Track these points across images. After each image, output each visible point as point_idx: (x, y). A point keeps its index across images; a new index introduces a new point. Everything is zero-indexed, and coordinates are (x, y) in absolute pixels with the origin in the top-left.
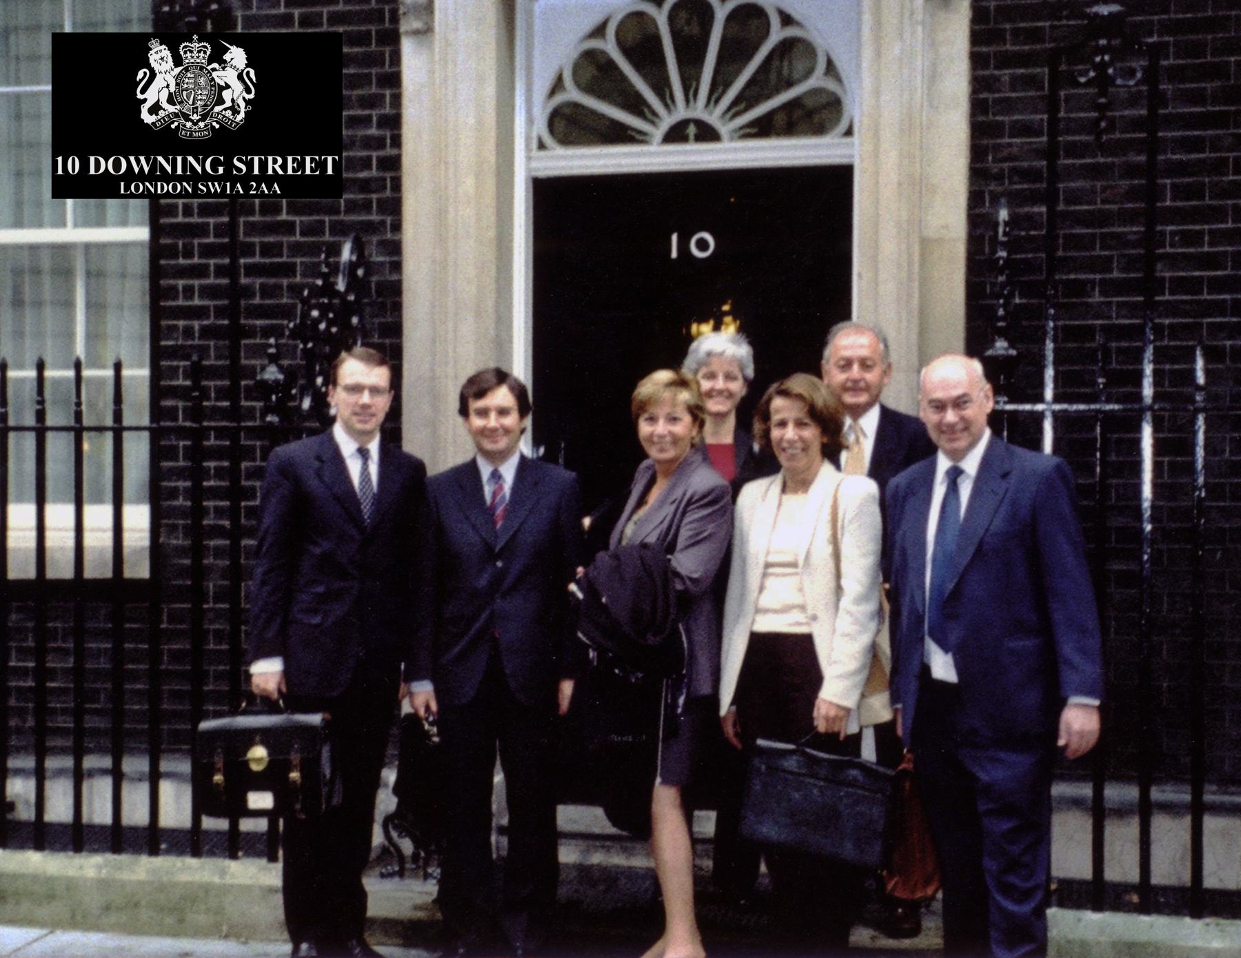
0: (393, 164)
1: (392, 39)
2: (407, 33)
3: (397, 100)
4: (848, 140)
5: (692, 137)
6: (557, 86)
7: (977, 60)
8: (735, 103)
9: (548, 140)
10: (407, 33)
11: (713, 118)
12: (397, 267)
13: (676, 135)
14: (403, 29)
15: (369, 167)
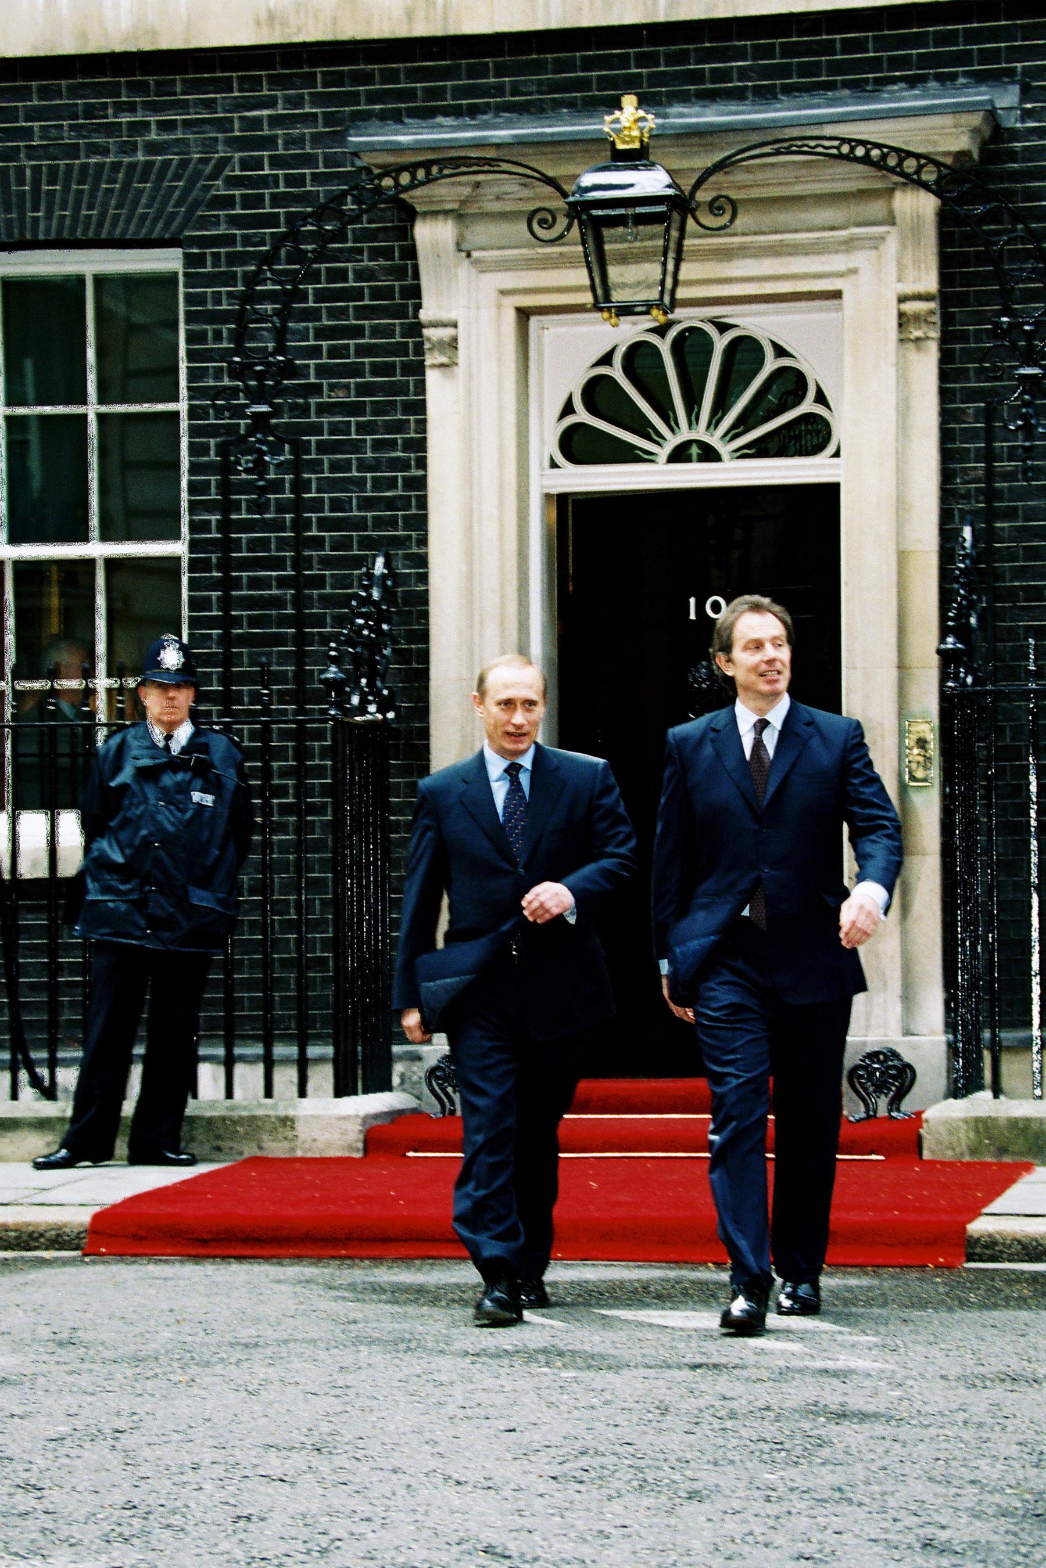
0: (421, 483)
1: (418, 369)
2: (433, 366)
3: (422, 426)
4: (835, 460)
5: (695, 457)
6: (568, 409)
7: (945, 395)
8: (734, 426)
9: (560, 459)
10: (433, 366)
11: (714, 440)
12: (424, 578)
13: (679, 455)
14: (427, 363)
15: (396, 487)
